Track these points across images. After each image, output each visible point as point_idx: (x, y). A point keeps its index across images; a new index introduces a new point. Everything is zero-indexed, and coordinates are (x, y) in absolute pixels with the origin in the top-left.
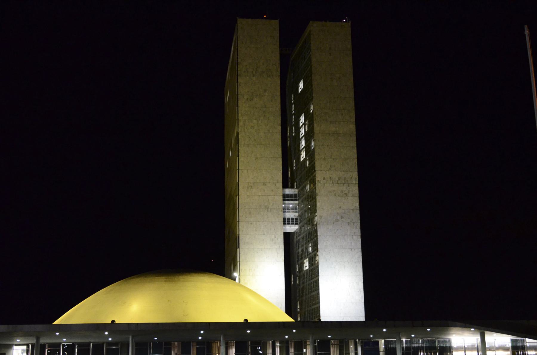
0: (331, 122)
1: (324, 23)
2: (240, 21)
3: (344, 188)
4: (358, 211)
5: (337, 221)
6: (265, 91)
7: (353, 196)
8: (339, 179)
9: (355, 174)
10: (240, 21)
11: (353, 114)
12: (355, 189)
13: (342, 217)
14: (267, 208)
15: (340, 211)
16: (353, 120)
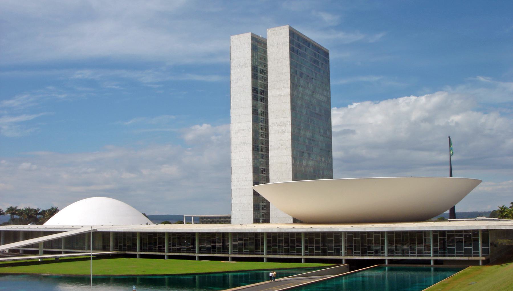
0: (277, 89)
1: (274, 29)
2: (231, 37)
3: (283, 128)
4: (291, 141)
5: (279, 148)
6: (244, 76)
7: (288, 132)
8: (281, 122)
9: (289, 119)
10: (231, 37)
11: (289, 82)
12: (289, 128)
13: (282, 145)
14: (244, 143)
15: (281, 142)
16: (289, 86)
